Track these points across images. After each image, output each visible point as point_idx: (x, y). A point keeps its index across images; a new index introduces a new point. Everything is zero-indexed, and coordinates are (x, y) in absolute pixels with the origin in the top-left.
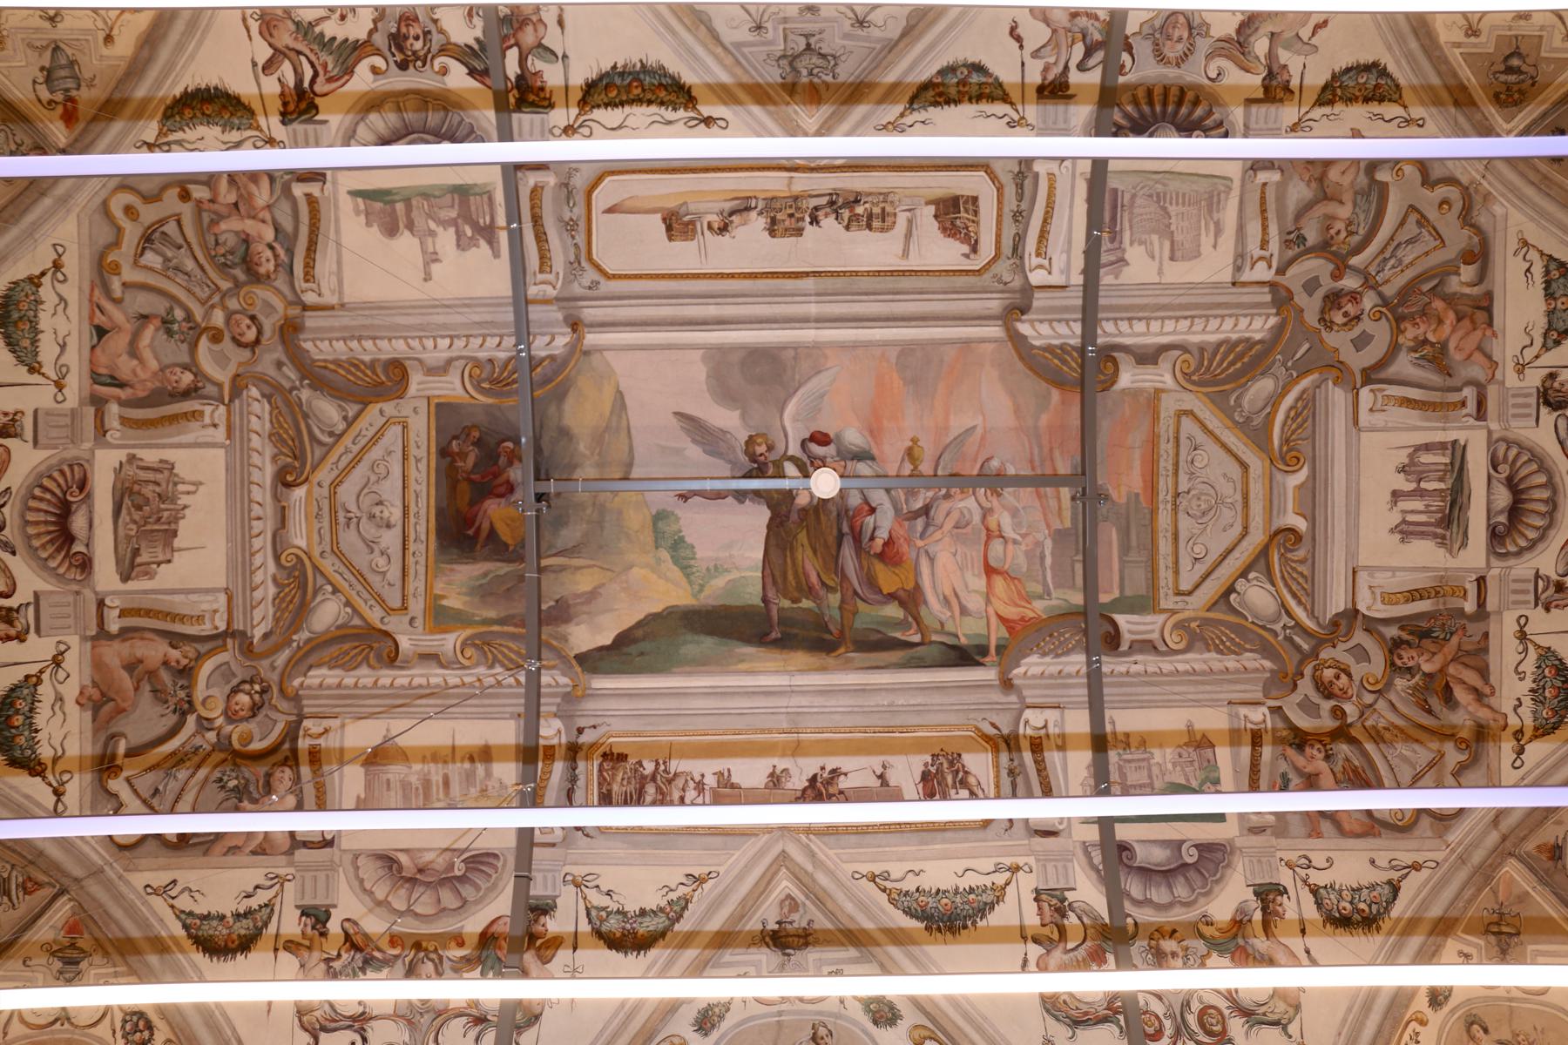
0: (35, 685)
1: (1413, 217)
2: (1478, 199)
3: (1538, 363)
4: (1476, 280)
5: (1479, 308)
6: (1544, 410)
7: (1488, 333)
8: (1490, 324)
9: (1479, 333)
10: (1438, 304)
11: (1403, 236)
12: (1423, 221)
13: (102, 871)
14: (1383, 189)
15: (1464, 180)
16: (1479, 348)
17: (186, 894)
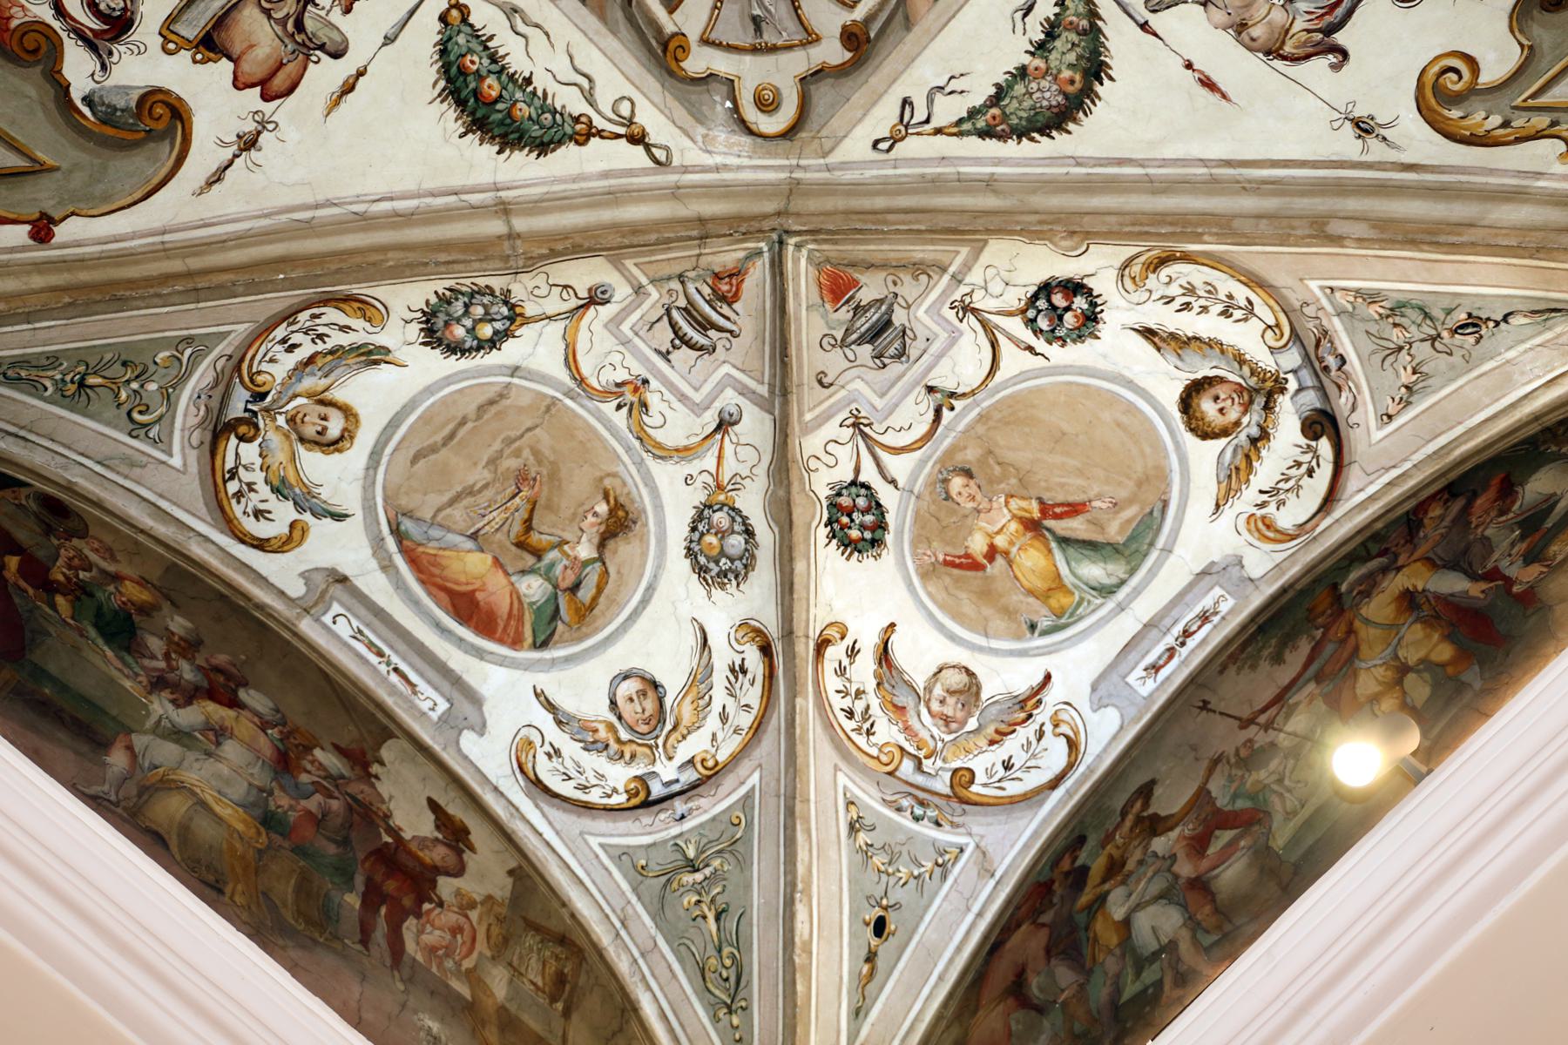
0: (464, 20)
13: (798, 182)
17: (939, 98)
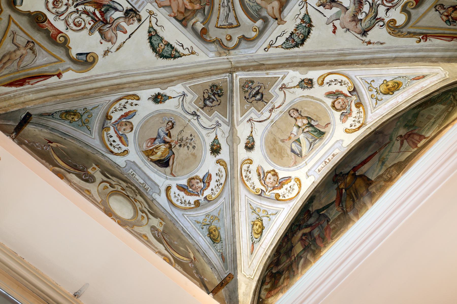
1: (235, 24)
2: (222, 51)
3: (148, 20)
4: (195, 26)
5: (184, 19)
6: (130, 7)
7: (173, 14)
8: (175, 17)
9: (175, 11)
10: (197, 6)
11: (232, 14)
12: (231, 26)
14: (254, 20)
15: (232, 52)
16: (170, 6)
